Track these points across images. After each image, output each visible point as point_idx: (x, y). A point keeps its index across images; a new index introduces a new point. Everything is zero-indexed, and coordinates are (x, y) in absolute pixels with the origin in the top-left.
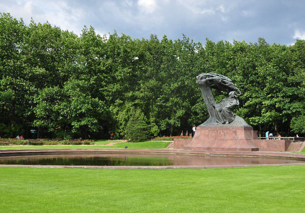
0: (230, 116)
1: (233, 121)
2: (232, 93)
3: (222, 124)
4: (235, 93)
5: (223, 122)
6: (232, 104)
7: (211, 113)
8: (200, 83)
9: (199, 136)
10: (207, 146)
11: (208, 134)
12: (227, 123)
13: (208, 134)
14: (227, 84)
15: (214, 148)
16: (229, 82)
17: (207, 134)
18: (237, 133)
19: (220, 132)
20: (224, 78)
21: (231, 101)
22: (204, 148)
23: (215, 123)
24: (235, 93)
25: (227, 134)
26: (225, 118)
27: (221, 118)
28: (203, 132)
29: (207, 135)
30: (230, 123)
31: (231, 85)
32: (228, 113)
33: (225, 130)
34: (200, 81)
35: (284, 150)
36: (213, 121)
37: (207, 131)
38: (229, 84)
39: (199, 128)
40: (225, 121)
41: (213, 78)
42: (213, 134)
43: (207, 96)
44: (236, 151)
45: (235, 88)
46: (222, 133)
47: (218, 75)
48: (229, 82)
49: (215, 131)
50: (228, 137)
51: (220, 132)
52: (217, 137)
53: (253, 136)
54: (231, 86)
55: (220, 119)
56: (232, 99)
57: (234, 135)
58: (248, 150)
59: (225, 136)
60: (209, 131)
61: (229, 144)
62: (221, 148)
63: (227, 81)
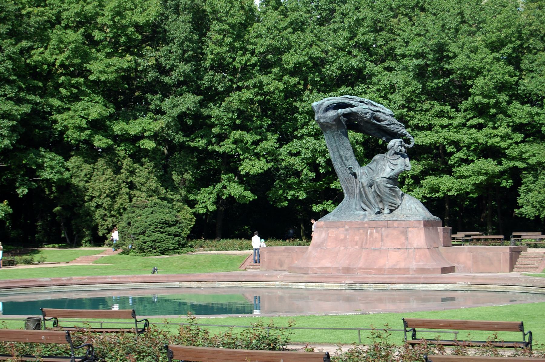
0: (393, 196)
1: (399, 206)
2: (394, 143)
3: (376, 214)
4: (401, 142)
5: (377, 210)
6: (397, 169)
7: (347, 189)
8: (322, 121)
9: (322, 243)
10: (343, 263)
11: (345, 238)
12: (386, 211)
13: (345, 238)
14: (383, 123)
15: (361, 268)
16: (387, 117)
17: (342, 237)
18: (410, 235)
19: (371, 234)
20: (378, 109)
22: (338, 269)
23: (358, 212)
24: (401, 142)
25: (387, 236)
26: (381, 201)
27: (372, 201)
28: (333, 232)
29: (342, 240)
30: (391, 211)
31: (392, 124)
32: (387, 190)
33: (383, 229)
34: (322, 116)
35: (508, 268)
36: (354, 207)
37: (343, 229)
39: (322, 223)
40: (381, 206)
41: (353, 109)
42: (357, 238)
43: (338, 151)
44: (409, 274)
45: (401, 131)
46: (376, 235)
48: (387, 117)
49: (361, 231)
50: (389, 244)
51: (371, 234)
52: (366, 243)
53: (441, 240)
54: (392, 126)
55: (370, 203)
56: (396, 157)
57: (403, 239)
58: (433, 271)
59: (382, 240)
60: (347, 230)
61: (392, 259)
62: (377, 269)
63: (383, 115)
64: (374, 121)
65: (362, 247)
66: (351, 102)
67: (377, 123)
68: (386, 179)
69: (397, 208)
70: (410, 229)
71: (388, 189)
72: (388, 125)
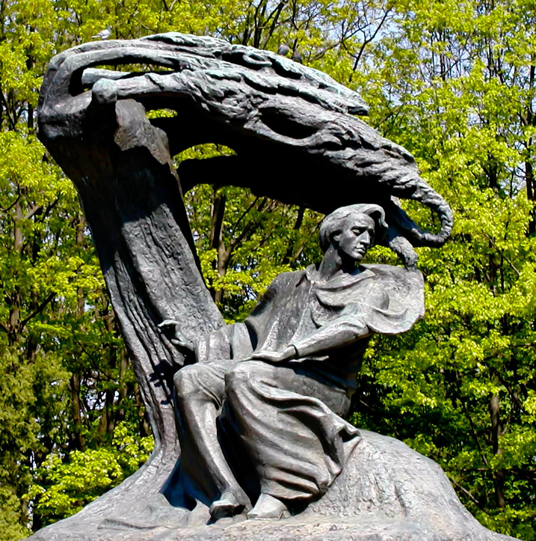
0: (297, 439)
4: (375, 215)
8: (53, 132)
16: (325, 115)
20: (286, 82)
21: (330, 299)
24: (375, 215)
32: (271, 415)
38: (324, 136)
41: (168, 81)
45: (389, 175)
47: (236, 58)
48: (325, 115)
54: (349, 152)
64: (264, 130)
66: (181, 56)
67: (279, 137)
68: (270, 368)
69: (317, 497)
71: (273, 411)
72: (330, 146)
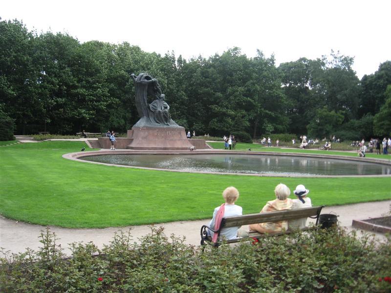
8: (143, 83)
9: (147, 136)
13: (157, 135)
17: (156, 134)
25: (174, 134)
29: (156, 136)
43: (143, 97)
46: (170, 134)
55: (162, 121)
57: (180, 136)
60: (158, 131)
65: (165, 139)
70: (182, 132)
